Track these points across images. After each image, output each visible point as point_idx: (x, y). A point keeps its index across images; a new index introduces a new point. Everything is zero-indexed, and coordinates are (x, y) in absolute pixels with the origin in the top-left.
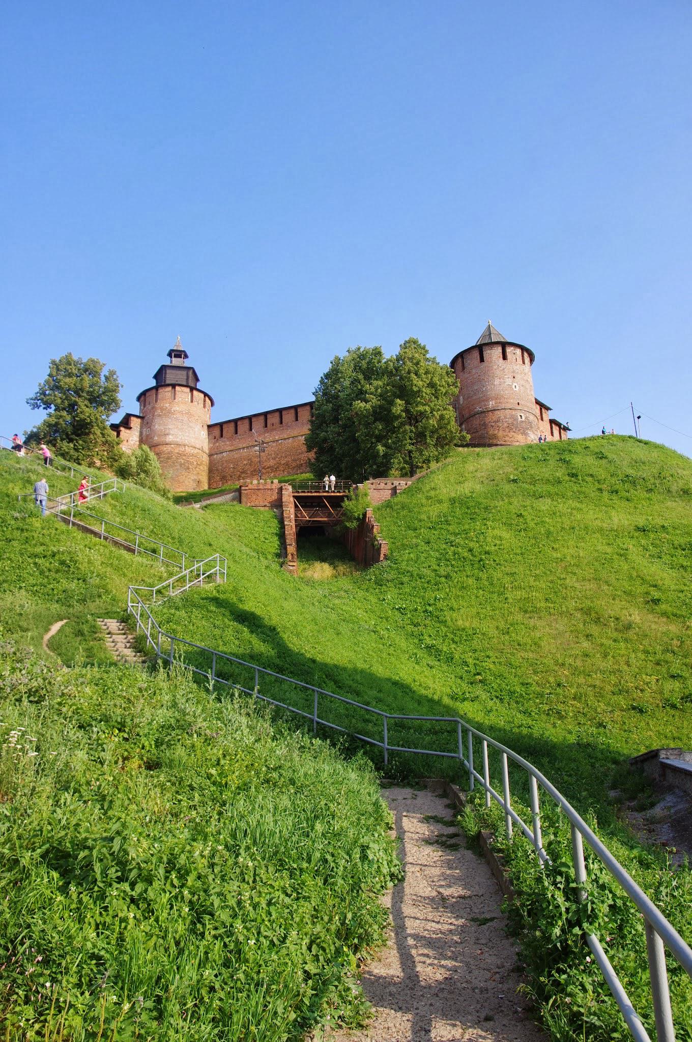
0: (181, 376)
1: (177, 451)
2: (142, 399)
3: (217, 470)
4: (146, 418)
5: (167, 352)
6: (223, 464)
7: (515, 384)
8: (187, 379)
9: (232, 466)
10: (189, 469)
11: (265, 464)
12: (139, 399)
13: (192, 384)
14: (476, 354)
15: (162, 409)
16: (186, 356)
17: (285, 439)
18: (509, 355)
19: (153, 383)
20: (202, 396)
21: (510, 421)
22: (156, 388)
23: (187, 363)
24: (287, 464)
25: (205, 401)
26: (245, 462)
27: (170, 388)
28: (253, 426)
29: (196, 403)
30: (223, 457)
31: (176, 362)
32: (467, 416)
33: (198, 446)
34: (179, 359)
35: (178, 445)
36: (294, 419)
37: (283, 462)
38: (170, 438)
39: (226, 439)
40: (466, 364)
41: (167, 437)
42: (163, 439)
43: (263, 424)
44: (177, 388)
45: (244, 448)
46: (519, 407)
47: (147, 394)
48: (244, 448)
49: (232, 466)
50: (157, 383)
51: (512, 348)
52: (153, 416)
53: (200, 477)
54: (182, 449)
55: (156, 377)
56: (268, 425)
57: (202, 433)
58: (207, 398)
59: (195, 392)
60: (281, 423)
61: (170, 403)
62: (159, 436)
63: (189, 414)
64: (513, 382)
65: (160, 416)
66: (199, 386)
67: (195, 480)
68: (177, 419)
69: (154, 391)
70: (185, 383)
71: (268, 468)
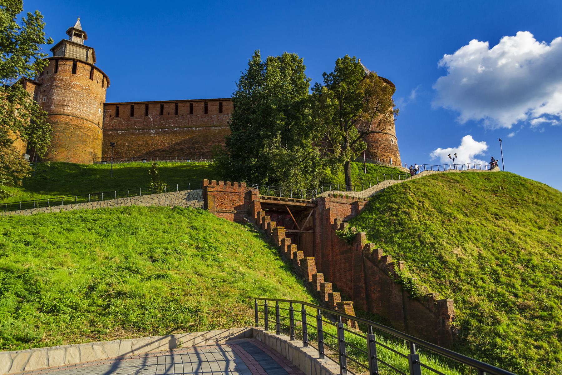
10: (85, 141)
15: (61, 81)
20: (101, 76)
28: (149, 112)
29: (96, 82)
33: (95, 121)
35: (76, 117)
36: (189, 112)
38: (68, 110)
41: (66, 108)
42: (61, 110)
43: (159, 112)
52: (52, 85)
53: (96, 151)
54: (80, 122)
56: (164, 113)
57: (100, 110)
60: (177, 113)
61: (70, 77)
62: (57, 105)
63: (89, 90)
65: (58, 86)
67: (91, 153)
68: (77, 93)
71: (163, 151)
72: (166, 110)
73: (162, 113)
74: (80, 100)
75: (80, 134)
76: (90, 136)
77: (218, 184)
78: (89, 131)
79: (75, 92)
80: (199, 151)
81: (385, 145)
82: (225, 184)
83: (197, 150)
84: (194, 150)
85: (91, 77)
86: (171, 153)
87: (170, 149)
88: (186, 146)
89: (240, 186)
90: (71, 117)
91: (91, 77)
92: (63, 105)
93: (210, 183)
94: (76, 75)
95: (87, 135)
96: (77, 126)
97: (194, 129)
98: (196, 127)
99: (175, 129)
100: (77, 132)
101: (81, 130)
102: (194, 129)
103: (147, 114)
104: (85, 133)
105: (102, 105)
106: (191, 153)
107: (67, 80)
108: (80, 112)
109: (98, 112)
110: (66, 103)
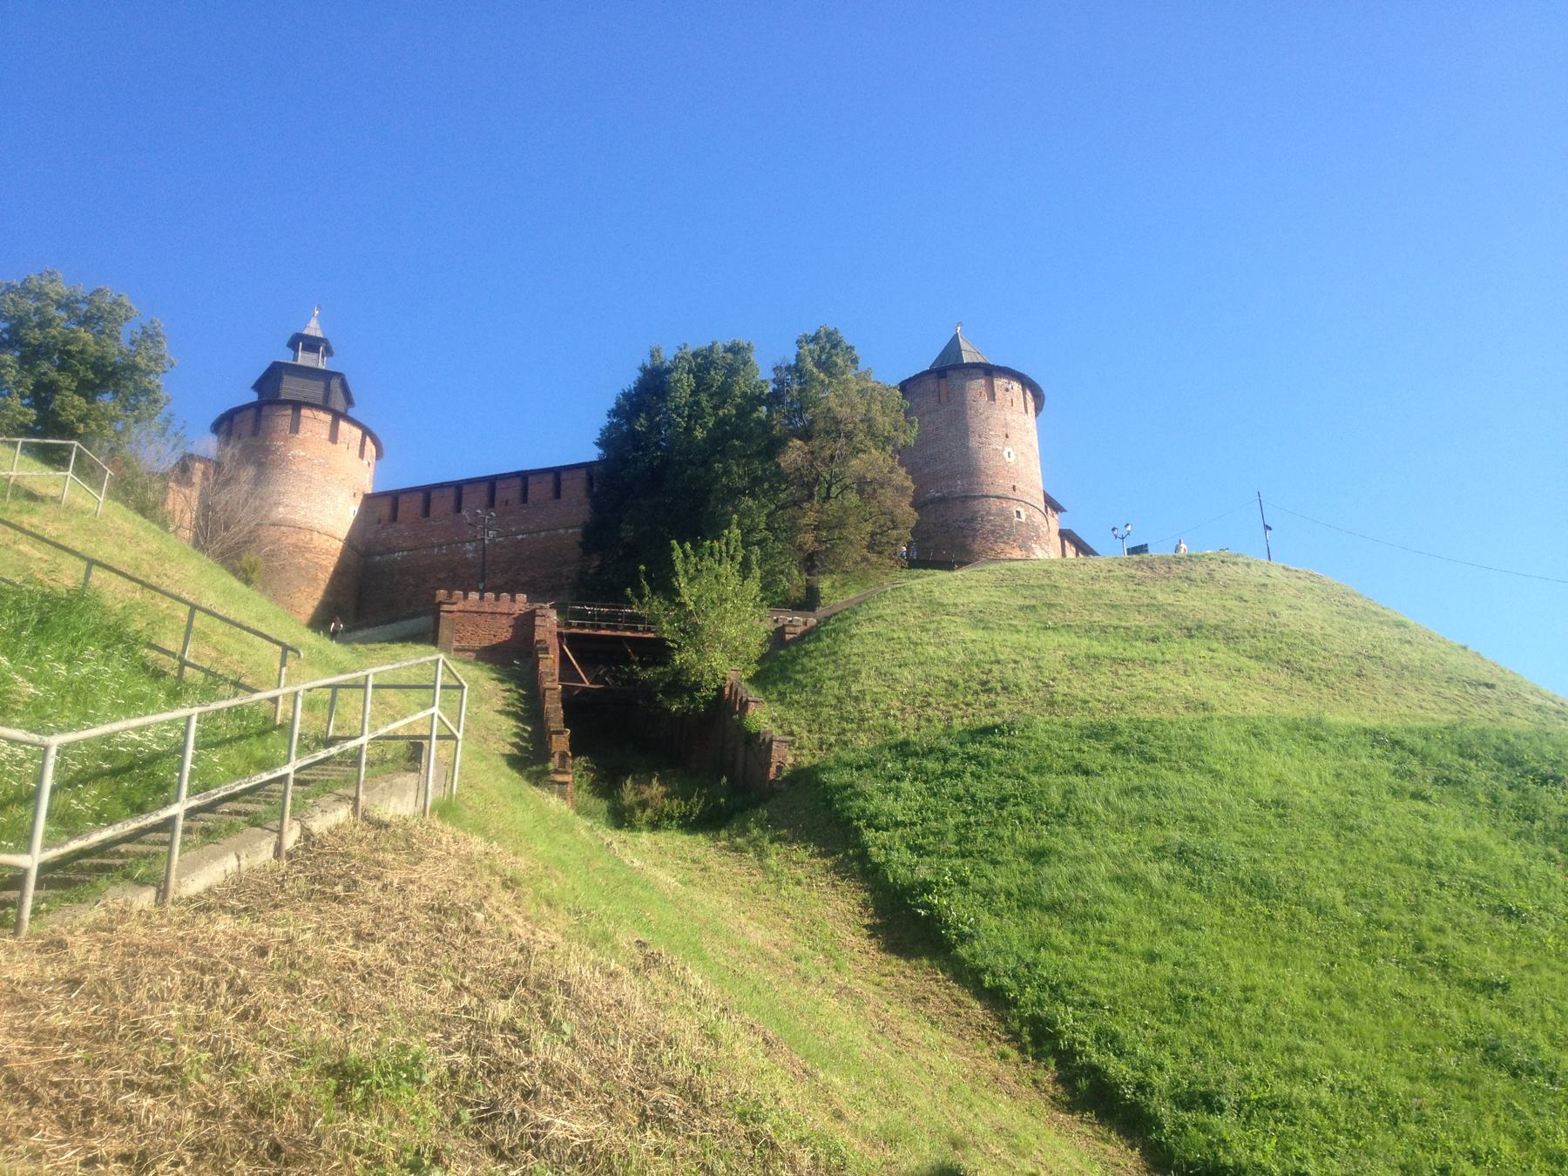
2: (224, 427)
5: (288, 338)
16: (329, 352)
18: (999, 393)
19: (253, 397)
20: (358, 433)
22: (257, 407)
31: (305, 359)
34: (313, 356)
36: (551, 495)
47: (237, 419)
48: (440, 546)
55: (258, 386)
56: (497, 503)
58: (368, 440)
59: (343, 425)
64: (1005, 444)
66: (352, 412)
69: (252, 413)
72: (499, 496)
75: (303, 563)
77: (466, 597)
82: (482, 598)
85: (333, 438)
89: (513, 600)
90: (283, 528)
91: (333, 438)
93: (450, 595)
94: (300, 436)
97: (562, 531)
98: (567, 528)
99: (520, 537)
102: (562, 531)
103: (458, 509)
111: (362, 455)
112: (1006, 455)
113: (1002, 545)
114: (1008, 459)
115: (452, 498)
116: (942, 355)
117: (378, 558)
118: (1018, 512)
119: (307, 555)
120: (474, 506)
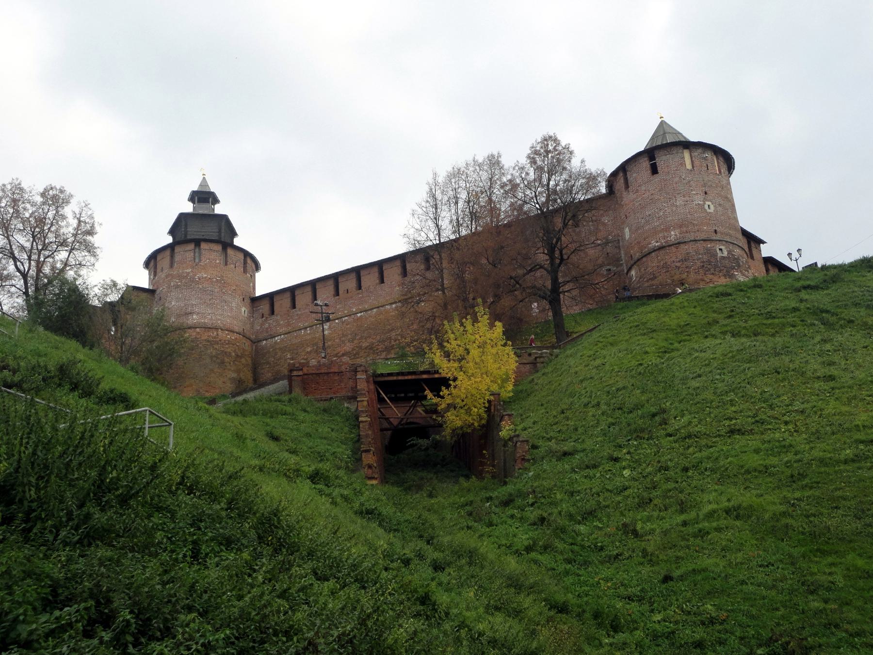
0: (210, 230)
1: (205, 337)
2: (152, 264)
3: (268, 363)
4: (158, 292)
5: (187, 195)
6: (276, 354)
7: (709, 203)
8: (220, 232)
9: (289, 356)
10: (223, 362)
11: (339, 349)
12: (147, 264)
13: (225, 238)
14: (645, 164)
16: (216, 201)
17: (366, 311)
19: (169, 240)
20: (241, 256)
21: (705, 258)
23: (219, 209)
24: (371, 348)
25: (245, 263)
26: (309, 349)
27: (191, 246)
28: (318, 296)
30: (276, 342)
31: (203, 209)
32: (638, 255)
33: (236, 329)
34: (204, 205)
35: (207, 328)
37: (364, 345)
38: (194, 319)
39: (279, 317)
40: (631, 179)
44: (204, 246)
45: (306, 328)
46: (718, 237)
47: (159, 258)
48: (306, 328)
49: (289, 356)
50: (173, 240)
51: (700, 151)
55: (172, 232)
56: (340, 292)
57: (243, 309)
58: (249, 261)
59: (230, 251)
60: (359, 287)
64: (705, 200)
66: (237, 242)
69: (168, 252)
70: (215, 237)
73: (337, 293)
74: (210, 300)
76: (230, 353)
78: (227, 346)
79: (201, 289)
80: (397, 342)
81: (703, 262)
83: (395, 341)
84: (390, 342)
86: (355, 355)
87: (353, 349)
88: (378, 337)
90: (198, 330)
92: (186, 314)
95: (226, 353)
96: (208, 341)
97: (388, 307)
99: (359, 315)
100: (209, 351)
101: (215, 346)
104: (222, 349)
105: (248, 301)
106: (386, 348)
107: (188, 273)
108: (211, 319)
109: (241, 313)
110: (189, 310)
111: (245, 271)
112: (706, 207)
113: (711, 276)
114: (708, 211)
115: (310, 293)
116: (653, 138)
117: (265, 342)
118: (721, 249)
119: (215, 346)
120: (325, 295)
